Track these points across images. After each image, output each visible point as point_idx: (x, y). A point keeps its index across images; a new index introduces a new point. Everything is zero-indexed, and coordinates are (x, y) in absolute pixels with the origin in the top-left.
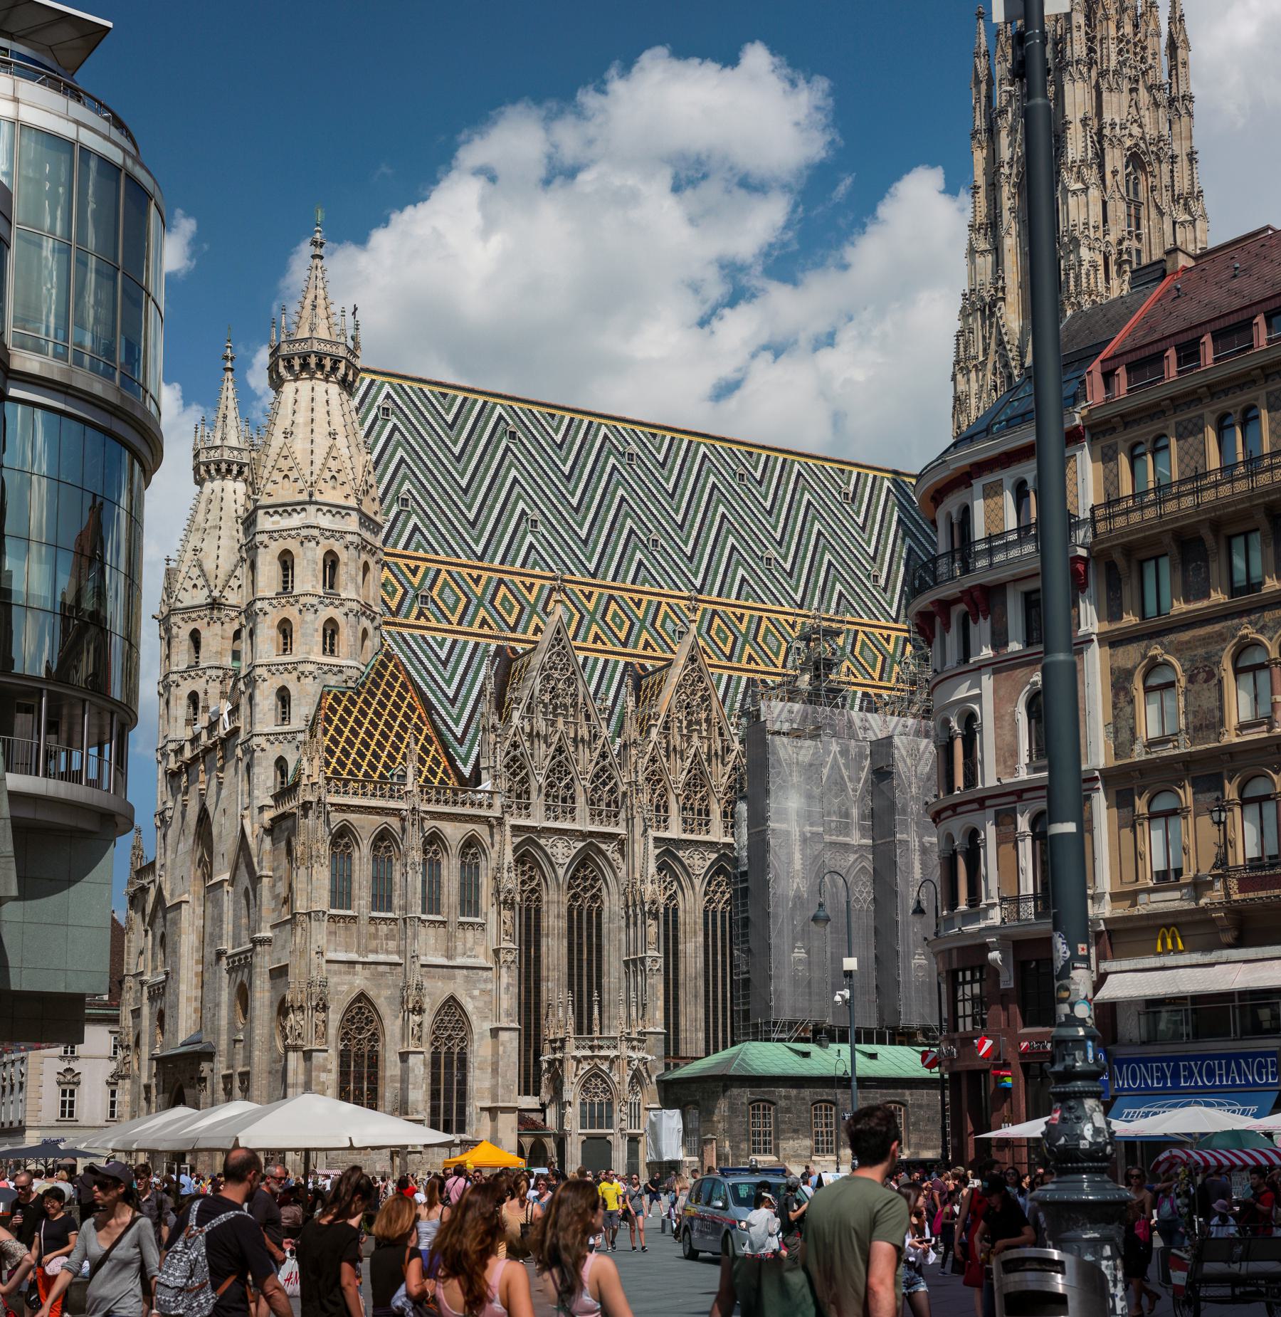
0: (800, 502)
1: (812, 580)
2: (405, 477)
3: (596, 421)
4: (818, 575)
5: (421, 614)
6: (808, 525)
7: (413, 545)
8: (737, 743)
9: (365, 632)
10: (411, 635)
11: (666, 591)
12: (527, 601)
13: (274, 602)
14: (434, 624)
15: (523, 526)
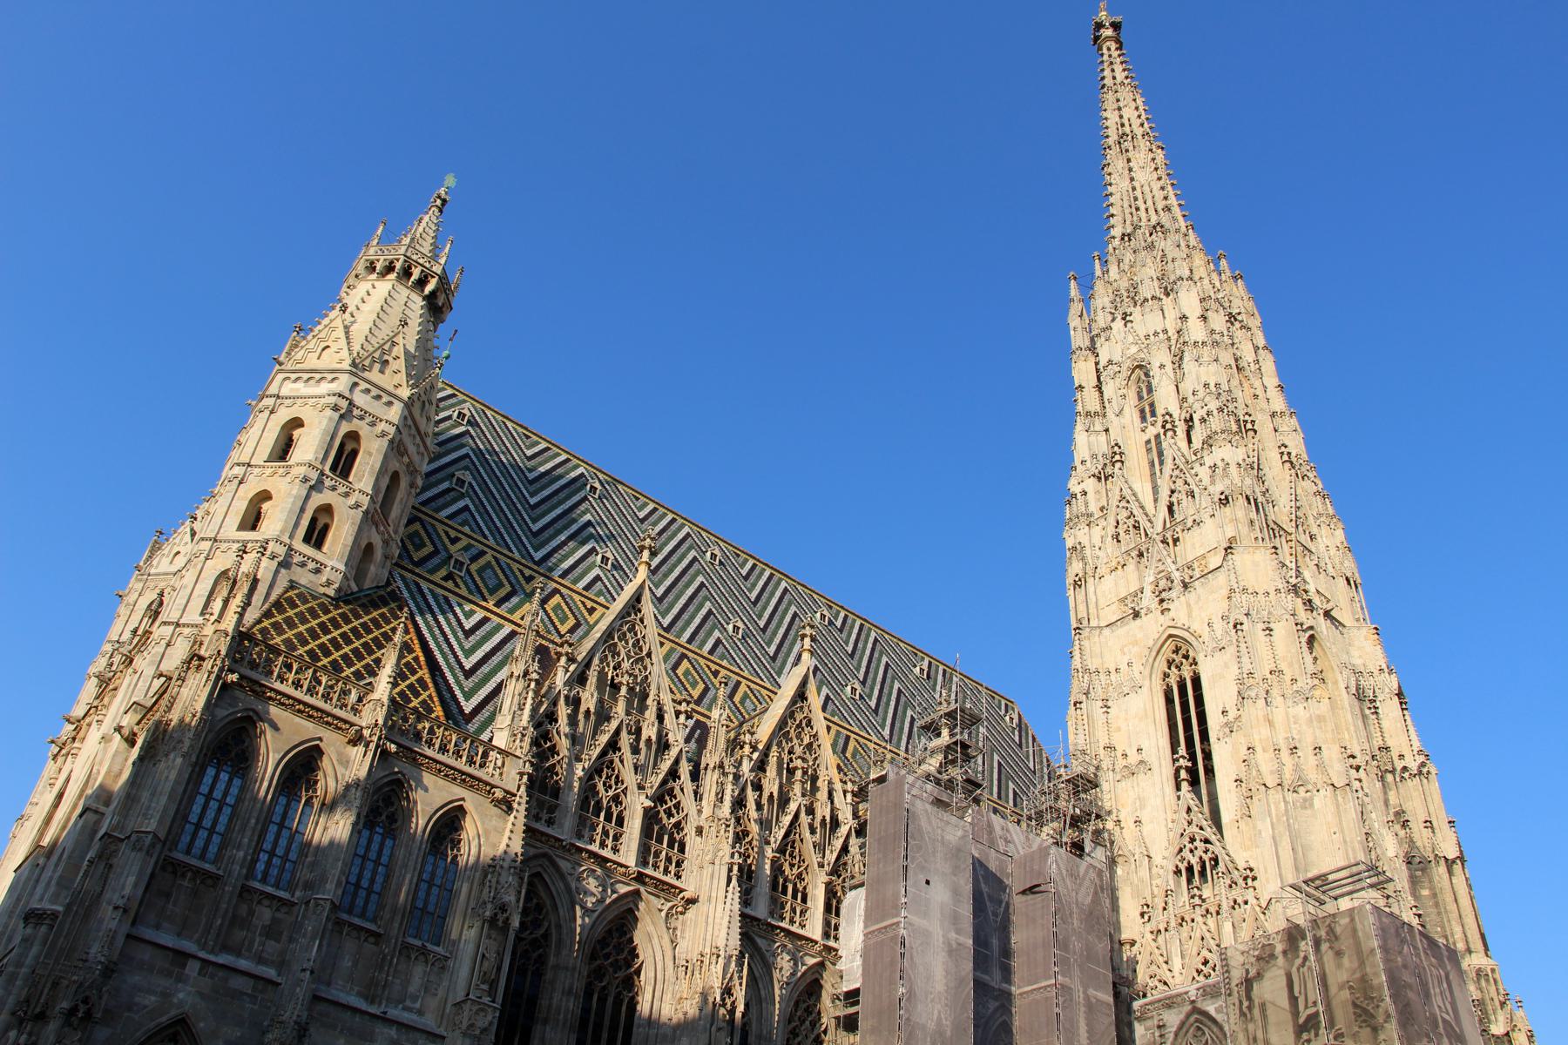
0: (879, 661)
1: (897, 725)
2: (466, 468)
3: (680, 521)
4: (903, 723)
5: (449, 577)
6: (888, 681)
7: (460, 518)
8: (850, 816)
9: (369, 548)
10: (431, 591)
11: (746, 674)
12: (586, 620)
13: (256, 471)
14: (464, 592)
15: (590, 559)
